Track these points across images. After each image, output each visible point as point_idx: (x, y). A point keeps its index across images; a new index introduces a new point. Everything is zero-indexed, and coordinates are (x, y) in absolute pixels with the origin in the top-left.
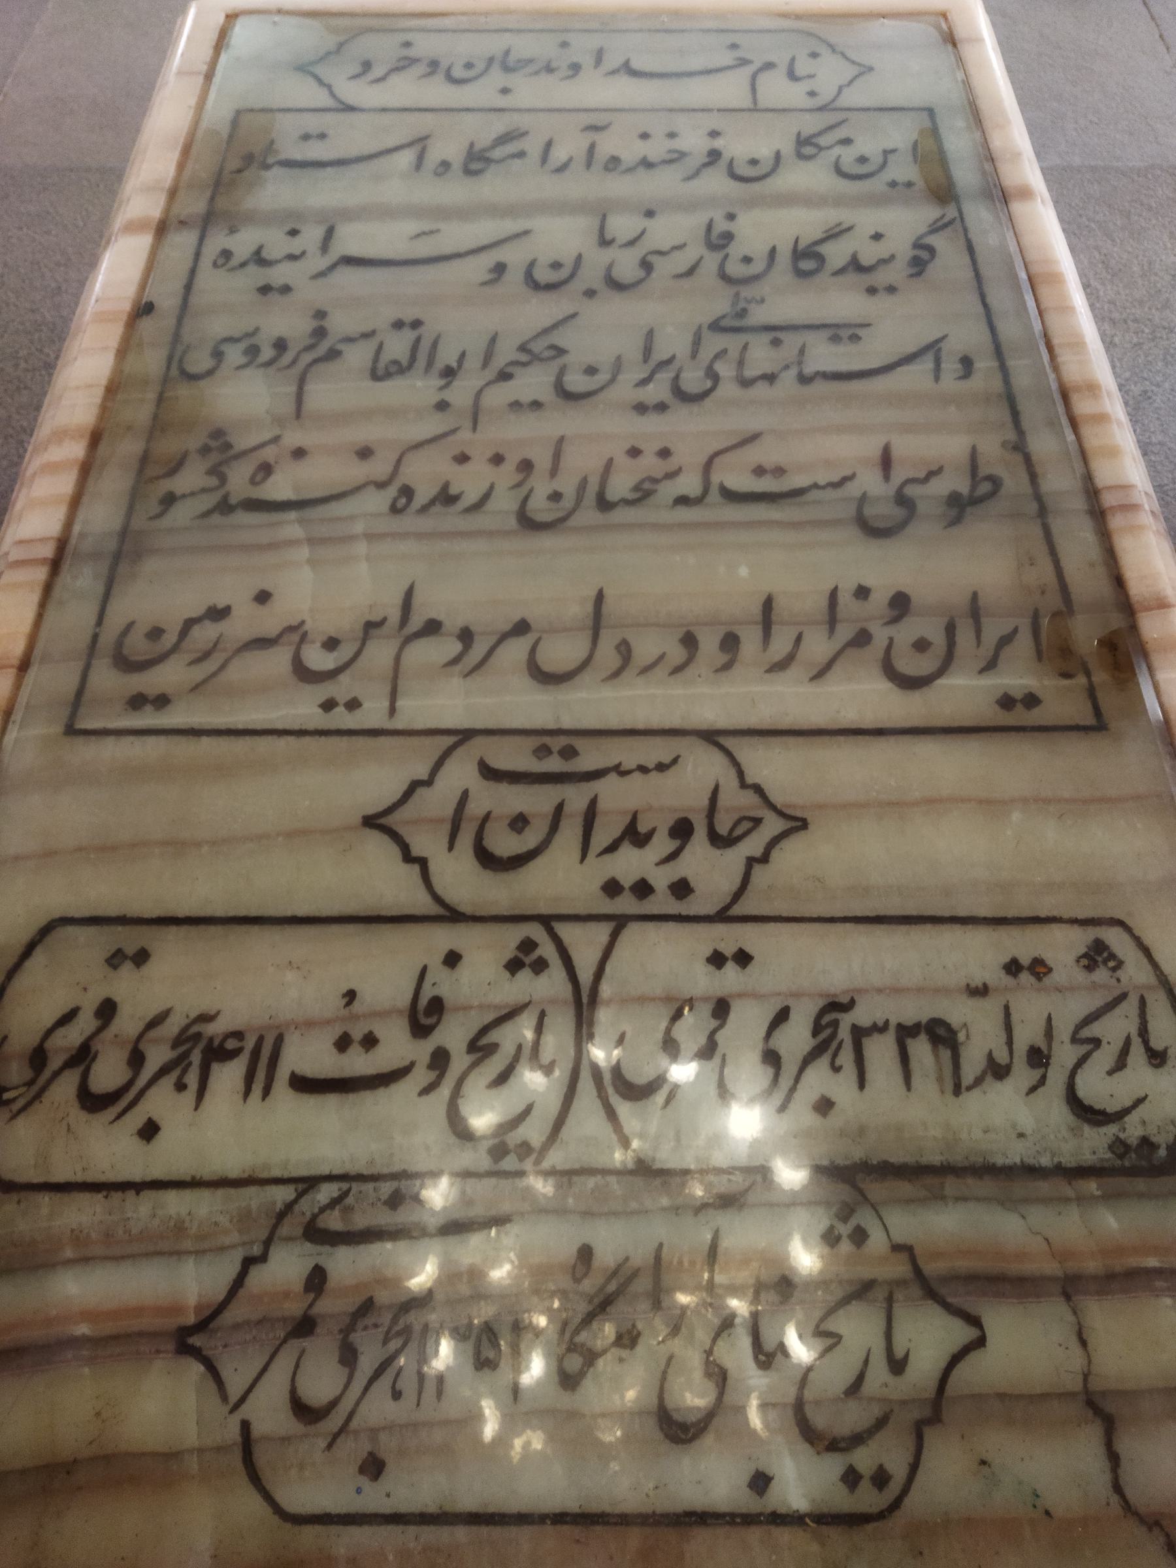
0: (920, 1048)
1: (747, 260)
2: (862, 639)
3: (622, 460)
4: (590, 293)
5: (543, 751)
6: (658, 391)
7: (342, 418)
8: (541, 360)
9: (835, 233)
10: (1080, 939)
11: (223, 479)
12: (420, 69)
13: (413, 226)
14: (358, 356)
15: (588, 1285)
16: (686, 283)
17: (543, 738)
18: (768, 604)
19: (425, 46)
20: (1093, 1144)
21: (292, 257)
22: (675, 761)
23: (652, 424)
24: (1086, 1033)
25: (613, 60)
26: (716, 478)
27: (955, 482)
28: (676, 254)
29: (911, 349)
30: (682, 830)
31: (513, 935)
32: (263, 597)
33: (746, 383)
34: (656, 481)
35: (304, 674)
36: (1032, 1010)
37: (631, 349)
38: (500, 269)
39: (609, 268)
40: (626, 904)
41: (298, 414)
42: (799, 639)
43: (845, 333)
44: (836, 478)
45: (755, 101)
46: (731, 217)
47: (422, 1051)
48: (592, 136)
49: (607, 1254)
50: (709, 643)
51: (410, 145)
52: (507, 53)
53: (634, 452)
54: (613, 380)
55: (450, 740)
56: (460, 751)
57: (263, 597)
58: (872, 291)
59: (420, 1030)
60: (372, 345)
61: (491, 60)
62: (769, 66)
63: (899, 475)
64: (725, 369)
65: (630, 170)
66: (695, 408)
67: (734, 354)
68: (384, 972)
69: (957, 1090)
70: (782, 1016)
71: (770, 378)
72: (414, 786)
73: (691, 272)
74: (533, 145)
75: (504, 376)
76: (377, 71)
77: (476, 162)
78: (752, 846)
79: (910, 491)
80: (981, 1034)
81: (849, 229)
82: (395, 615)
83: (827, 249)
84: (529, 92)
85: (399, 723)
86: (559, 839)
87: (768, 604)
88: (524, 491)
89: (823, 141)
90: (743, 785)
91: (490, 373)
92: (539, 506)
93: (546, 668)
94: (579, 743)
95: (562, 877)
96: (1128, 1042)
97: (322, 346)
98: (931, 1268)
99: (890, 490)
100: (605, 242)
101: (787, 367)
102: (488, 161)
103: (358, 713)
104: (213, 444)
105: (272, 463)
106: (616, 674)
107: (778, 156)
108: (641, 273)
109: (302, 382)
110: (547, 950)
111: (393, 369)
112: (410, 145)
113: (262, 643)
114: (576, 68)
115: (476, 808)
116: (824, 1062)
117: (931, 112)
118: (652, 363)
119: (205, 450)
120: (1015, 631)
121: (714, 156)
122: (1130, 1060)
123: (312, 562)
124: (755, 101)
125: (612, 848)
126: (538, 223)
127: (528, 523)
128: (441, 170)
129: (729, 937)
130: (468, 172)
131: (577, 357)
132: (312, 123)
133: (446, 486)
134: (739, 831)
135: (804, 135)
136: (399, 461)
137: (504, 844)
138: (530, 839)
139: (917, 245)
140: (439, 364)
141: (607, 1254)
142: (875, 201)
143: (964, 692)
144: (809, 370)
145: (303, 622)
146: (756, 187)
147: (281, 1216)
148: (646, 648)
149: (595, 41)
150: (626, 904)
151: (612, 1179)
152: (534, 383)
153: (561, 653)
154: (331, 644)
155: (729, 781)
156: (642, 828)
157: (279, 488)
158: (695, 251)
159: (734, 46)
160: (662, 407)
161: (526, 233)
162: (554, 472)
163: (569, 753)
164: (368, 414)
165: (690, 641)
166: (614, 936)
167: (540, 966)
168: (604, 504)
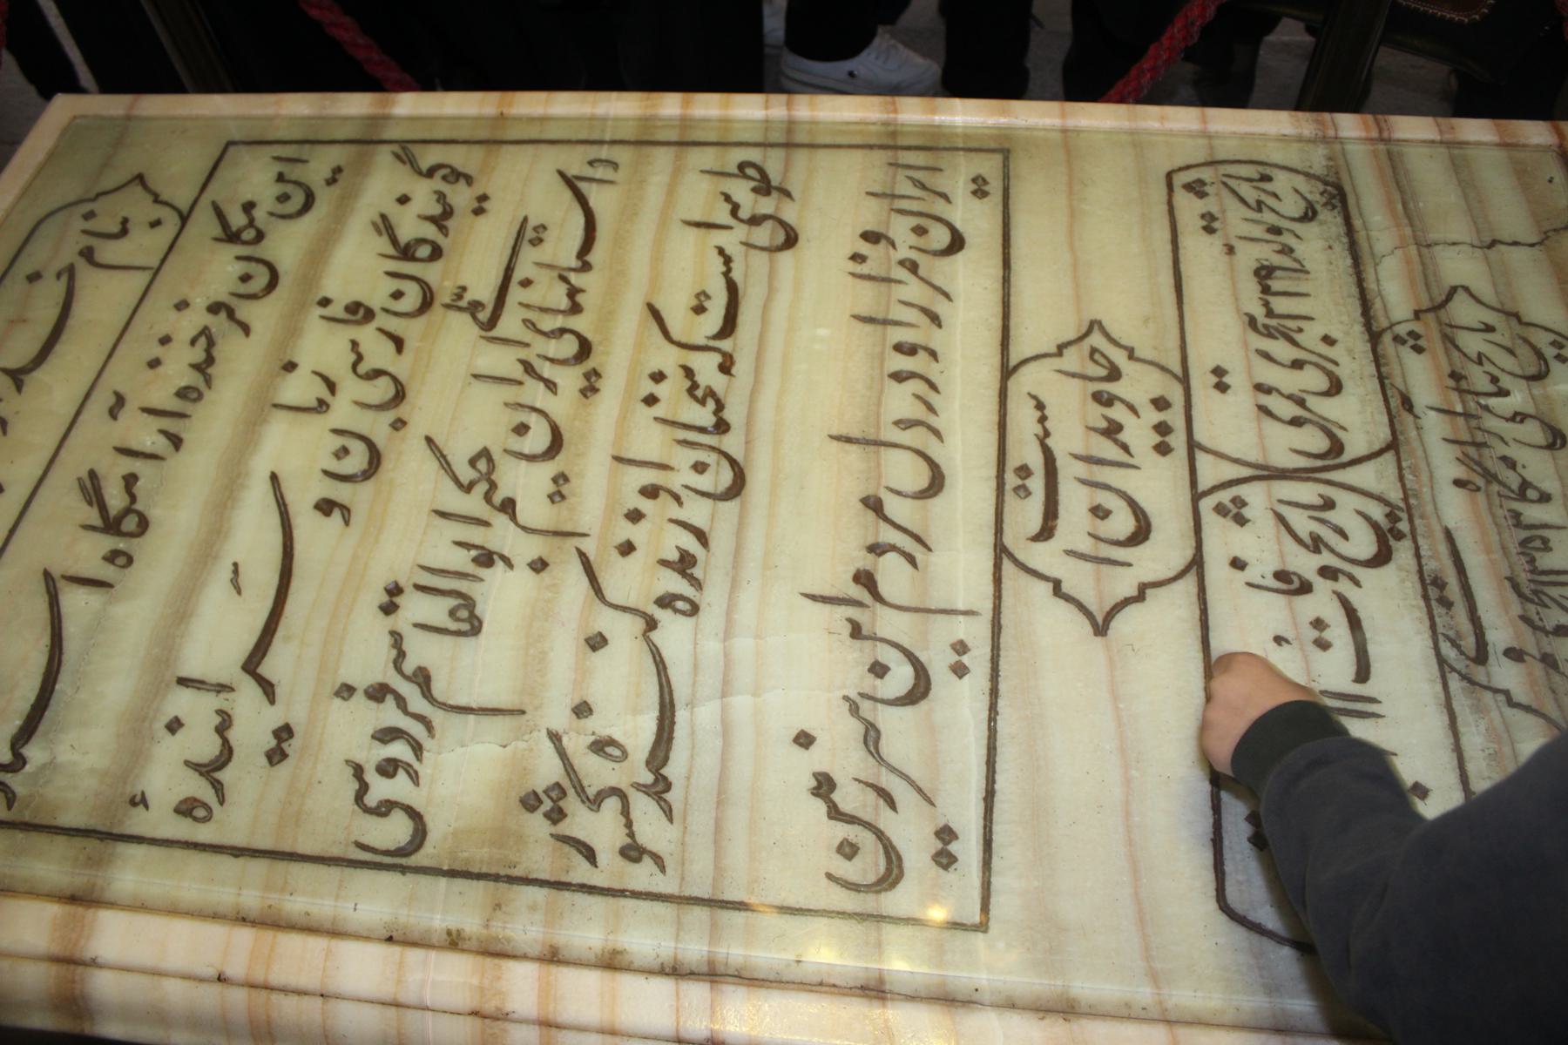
7: (534, 660)
15: (1480, 482)
33: (576, 309)
40: (1178, 440)
49: (1460, 472)
85: (986, 606)
86: (1114, 484)
91: (501, 520)
104: (547, 805)
105: (592, 738)
123: (756, 692)
136: (616, 607)
140: (471, 568)
141: (1460, 472)
147: (1472, 682)
150: (1178, 440)
167: (1239, 502)
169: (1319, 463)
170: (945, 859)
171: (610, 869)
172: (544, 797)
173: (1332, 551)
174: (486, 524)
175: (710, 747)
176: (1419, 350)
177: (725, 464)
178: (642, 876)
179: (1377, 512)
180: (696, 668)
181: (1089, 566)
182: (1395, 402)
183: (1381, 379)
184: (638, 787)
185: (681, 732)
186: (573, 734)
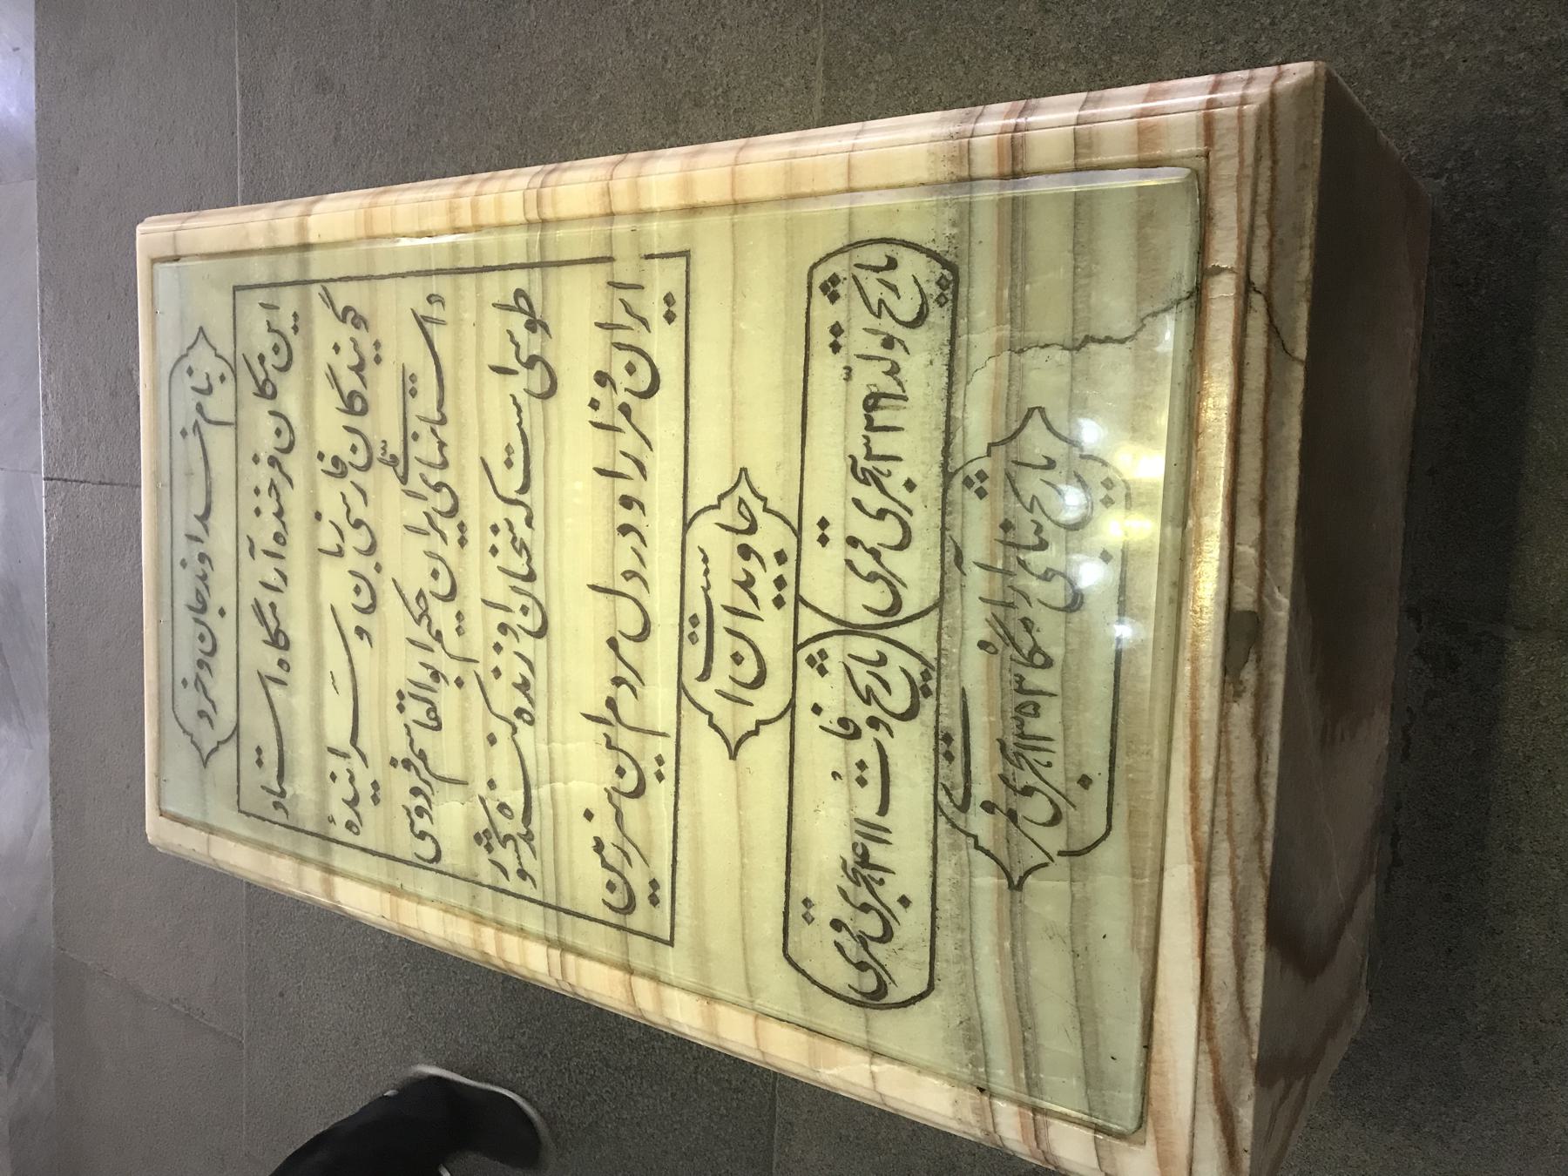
0: (880, 418)
1: (354, 449)
2: (625, 410)
3: (499, 560)
4: (378, 568)
6: (449, 528)
7: (466, 750)
9: (334, 380)
10: (820, 299)
11: (509, 837)
12: (204, 674)
13: (328, 690)
14: (424, 738)
15: (999, 644)
16: (371, 496)
17: (684, 638)
18: (601, 472)
19: (186, 668)
20: (939, 316)
21: (352, 779)
22: (702, 551)
23: (473, 534)
24: (875, 308)
25: (197, 529)
26: (514, 496)
27: (518, 321)
28: (349, 501)
29: (422, 339)
30: (745, 552)
31: (804, 670)
32: (589, 815)
33: (444, 464)
34: (514, 539)
35: (638, 792)
36: (860, 341)
37: (419, 544)
38: (360, 631)
39: (360, 552)
41: (465, 783)
42: (624, 454)
43: (409, 386)
46: (321, 456)
47: (867, 732)
49: (983, 633)
50: (626, 517)
51: (265, 687)
53: (494, 551)
54: (441, 559)
55: (684, 699)
56: (691, 693)
57: (589, 815)
58: (378, 360)
59: (857, 734)
60: (415, 729)
61: (197, 620)
63: (513, 364)
66: (462, 503)
67: (424, 469)
68: (822, 752)
69: (905, 399)
70: (858, 503)
71: (442, 445)
73: (363, 493)
74: (267, 597)
75: (438, 636)
76: (208, 707)
77: (278, 639)
78: (756, 506)
79: (524, 358)
80: (871, 376)
82: (603, 728)
84: (221, 595)
87: (601, 472)
88: (520, 632)
89: (262, 377)
90: (718, 507)
91: (437, 646)
94: (687, 616)
95: (771, 632)
96: (881, 281)
97: (415, 761)
98: (1003, 435)
100: (340, 553)
101: (433, 431)
102: (278, 631)
103: (665, 758)
104: (485, 841)
106: (645, 583)
107: (272, 413)
110: (813, 649)
111: (432, 715)
112: (265, 687)
113: (619, 816)
114: (203, 557)
115: (727, 686)
116: (885, 481)
117: (236, 289)
119: (489, 848)
121: (273, 461)
122: (893, 282)
125: (754, 599)
127: (542, 632)
129: (811, 532)
130: (287, 647)
131: (428, 585)
132: (249, 758)
133: (516, 685)
134: (746, 514)
135: (256, 389)
137: (749, 671)
138: (747, 652)
139: (344, 320)
140: (429, 681)
141: (983, 633)
142: (308, 347)
148: (631, 563)
150: (788, 594)
151: (944, 623)
152: (443, 615)
154: (620, 772)
155: (714, 516)
156: (743, 578)
157: (516, 801)
158: (345, 485)
161: (333, 609)
162: (507, 609)
163: (694, 620)
164: (465, 736)
165: (625, 530)
166: (807, 604)
167: (823, 654)
169: (881, 620)
170: (654, 900)
171: (514, 883)
173: (879, 703)
175: (549, 811)
176: (981, 493)
178: (526, 888)
179: (915, 669)
181: (729, 703)
182: (950, 556)
183: (944, 529)
185: (535, 804)
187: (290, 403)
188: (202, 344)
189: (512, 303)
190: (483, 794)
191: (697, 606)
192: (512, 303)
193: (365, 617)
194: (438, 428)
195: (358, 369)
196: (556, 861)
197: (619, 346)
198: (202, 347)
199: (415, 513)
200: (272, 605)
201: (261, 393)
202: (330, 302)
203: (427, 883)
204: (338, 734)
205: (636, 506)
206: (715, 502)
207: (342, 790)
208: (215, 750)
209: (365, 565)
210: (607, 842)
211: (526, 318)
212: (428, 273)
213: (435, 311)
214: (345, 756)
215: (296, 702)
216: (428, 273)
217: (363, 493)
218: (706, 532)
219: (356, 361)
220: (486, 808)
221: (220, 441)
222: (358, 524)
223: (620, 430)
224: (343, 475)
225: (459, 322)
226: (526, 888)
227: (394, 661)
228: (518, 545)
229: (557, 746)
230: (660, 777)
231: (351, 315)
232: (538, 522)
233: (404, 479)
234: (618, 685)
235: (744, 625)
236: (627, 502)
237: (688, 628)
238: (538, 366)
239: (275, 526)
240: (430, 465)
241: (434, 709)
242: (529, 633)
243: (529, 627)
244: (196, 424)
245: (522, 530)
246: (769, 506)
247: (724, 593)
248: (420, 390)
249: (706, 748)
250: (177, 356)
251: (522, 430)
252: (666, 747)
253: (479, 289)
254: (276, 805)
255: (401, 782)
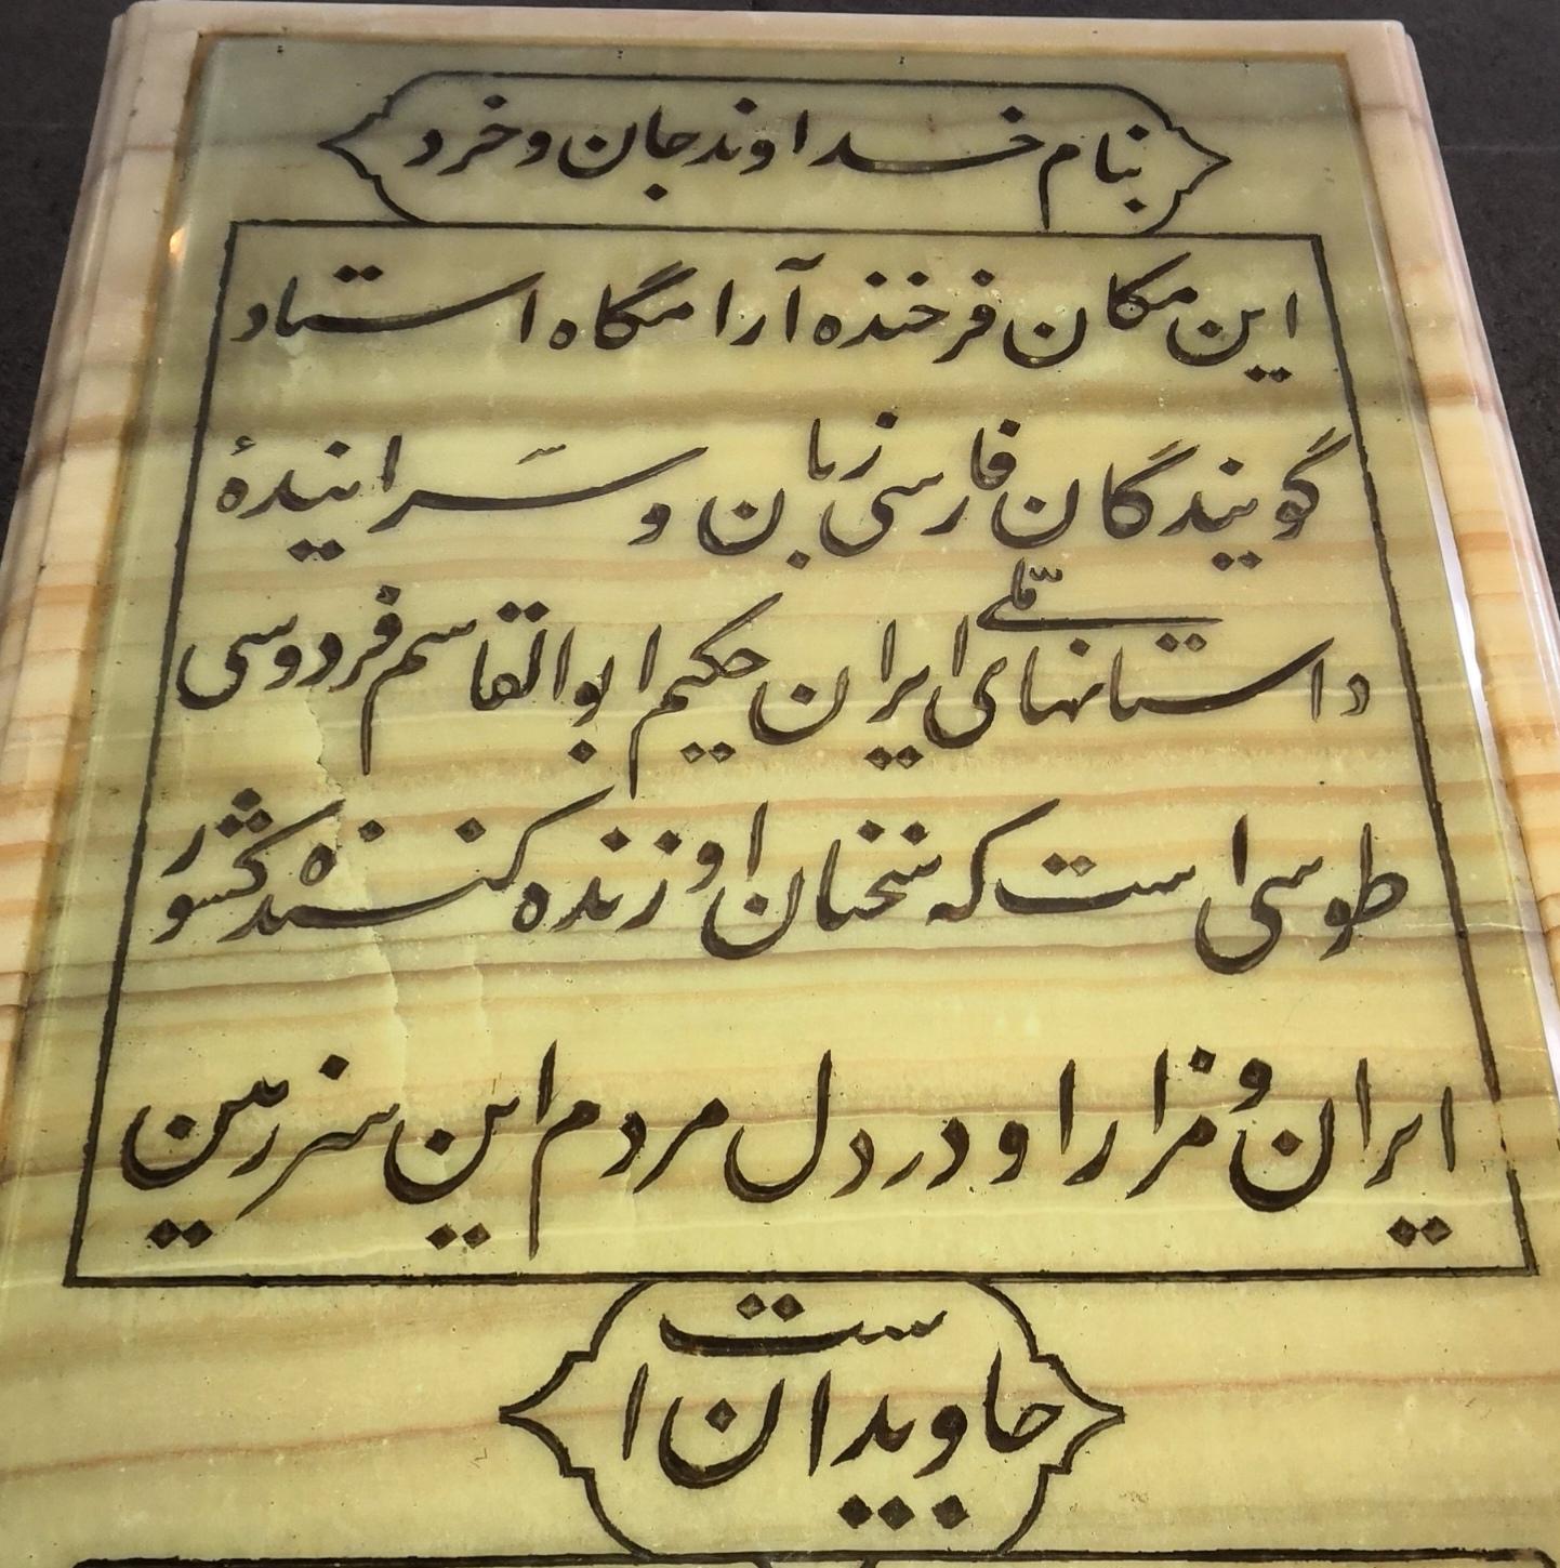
1: (1035, 505)
3: (853, 844)
4: (798, 560)
5: (750, 1307)
6: (903, 729)
7: (437, 768)
8: (729, 675)
9: (1172, 458)
11: (260, 875)
12: (518, 148)
13: (521, 440)
14: (450, 665)
16: (942, 543)
18: (1068, 1078)
19: (528, 105)
21: (338, 494)
22: (939, 1319)
23: (896, 780)
25: (823, 139)
26: (991, 876)
27: (1340, 881)
29: (1280, 662)
30: (950, 1425)
32: (334, 1067)
33: (1033, 715)
34: (902, 879)
35: (401, 1187)
38: (659, 517)
43: (1181, 634)
44: (1166, 878)
45: (1046, 220)
46: (1010, 428)
48: (794, 278)
50: (984, 1137)
52: (656, 119)
53: (871, 832)
57: (334, 1067)
58: (1222, 561)
60: (466, 648)
62: (1067, 153)
63: (1257, 872)
64: (1004, 692)
65: (857, 340)
66: (959, 756)
67: (1016, 667)
71: (1071, 709)
72: (570, 1360)
73: (948, 526)
76: (452, 152)
77: (616, 323)
78: (1047, 1448)
79: (1273, 897)
81: (1192, 451)
82: (530, 1096)
83: (1153, 487)
84: (696, 194)
87: (1068, 1078)
88: (710, 893)
89: (1152, 293)
90: (1035, 1357)
91: (652, 698)
92: (737, 925)
93: (753, 1175)
97: (398, 647)
99: (1246, 894)
101: (1095, 690)
102: (635, 322)
104: (243, 816)
105: (333, 847)
106: (853, 1186)
108: (875, 527)
109: (368, 713)
111: (505, 688)
114: (765, 151)
115: (659, 1394)
118: (896, 680)
119: (229, 826)
120: (1419, 1121)
121: (984, 317)
124: (1046, 220)
125: (853, 1452)
126: (717, 435)
127: (718, 947)
128: (561, 338)
130: (604, 343)
131: (781, 674)
133: (595, 885)
135: (1123, 282)
137: (701, 1446)
138: (739, 1437)
139: (1290, 483)
142: (1225, 402)
143: (1346, 1219)
144: (1127, 697)
145: (396, 1107)
146: (1048, 375)
148: (891, 1151)
149: (795, 101)
152: (718, 713)
153: (767, 1158)
154: (440, 1141)
155: (1016, 1350)
156: (895, 1422)
157: (344, 889)
158: (958, 485)
159: (1013, 115)
160: (911, 756)
161: (699, 452)
162: (753, 863)
164: (468, 764)
165: (957, 1136)
168: (828, 918)
171: (158, 888)
172: (254, 810)
174: (643, 684)
175: (330, 969)
177: (766, 933)
178: (152, 920)
180: (439, 940)
184: (269, 899)
185: (341, 935)
186: (338, 826)
187: (1110, 358)
188: (1199, 162)
189: (1377, 871)
190: (346, 811)
191: (822, 1313)
192: (1377, 871)
193: (693, 530)
194: (1103, 700)
195: (1196, 516)
196: (220, 990)
197: (1328, 1116)
198: (1199, 162)
199: (925, 647)
200: (685, 311)
201: (1119, 293)
202: (1323, 450)
203: (133, 674)
204: (438, 460)
205: (1010, 1160)
206: (1043, 1350)
207: (315, 471)
208: (361, 170)
209: (799, 531)
210: (278, 1113)
211: (1352, 899)
212: (1409, 676)
213: (1337, 695)
214: (388, 478)
215: (486, 360)
216: (1409, 676)
217: (948, 526)
218: (979, 1328)
219: (1214, 510)
220: (315, 818)
221: (1004, 195)
222: (883, 514)
223: (1159, 1120)
224: (978, 477)
225: (1324, 745)
226: (152, 920)
227: (613, 599)
228: (891, 886)
229: (476, 986)
230: (441, 1237)
231: (1302, 500)
232: (944, 931)
233: (988, 621)
234: (626, 1129)
235: (794, 1427)
236: (1014, 1139)
237: (771, 1293)
238: (1261, 931)
239: (854, 319)
240: (1027, 680)
241: (517, 693)
242: (711, 915)
243: (722, 918)
244: (1032, 144)
245: (923, 895)
246: (1055, 1480)
247: (859, 1375)
248: (1174, 659)
249: (518, 1350)
250: (1167, 104)
251: (1122, 895)
252: (505, 1251)
253: (1395, 792)
254: (259, 314)
255: (338, 606)
